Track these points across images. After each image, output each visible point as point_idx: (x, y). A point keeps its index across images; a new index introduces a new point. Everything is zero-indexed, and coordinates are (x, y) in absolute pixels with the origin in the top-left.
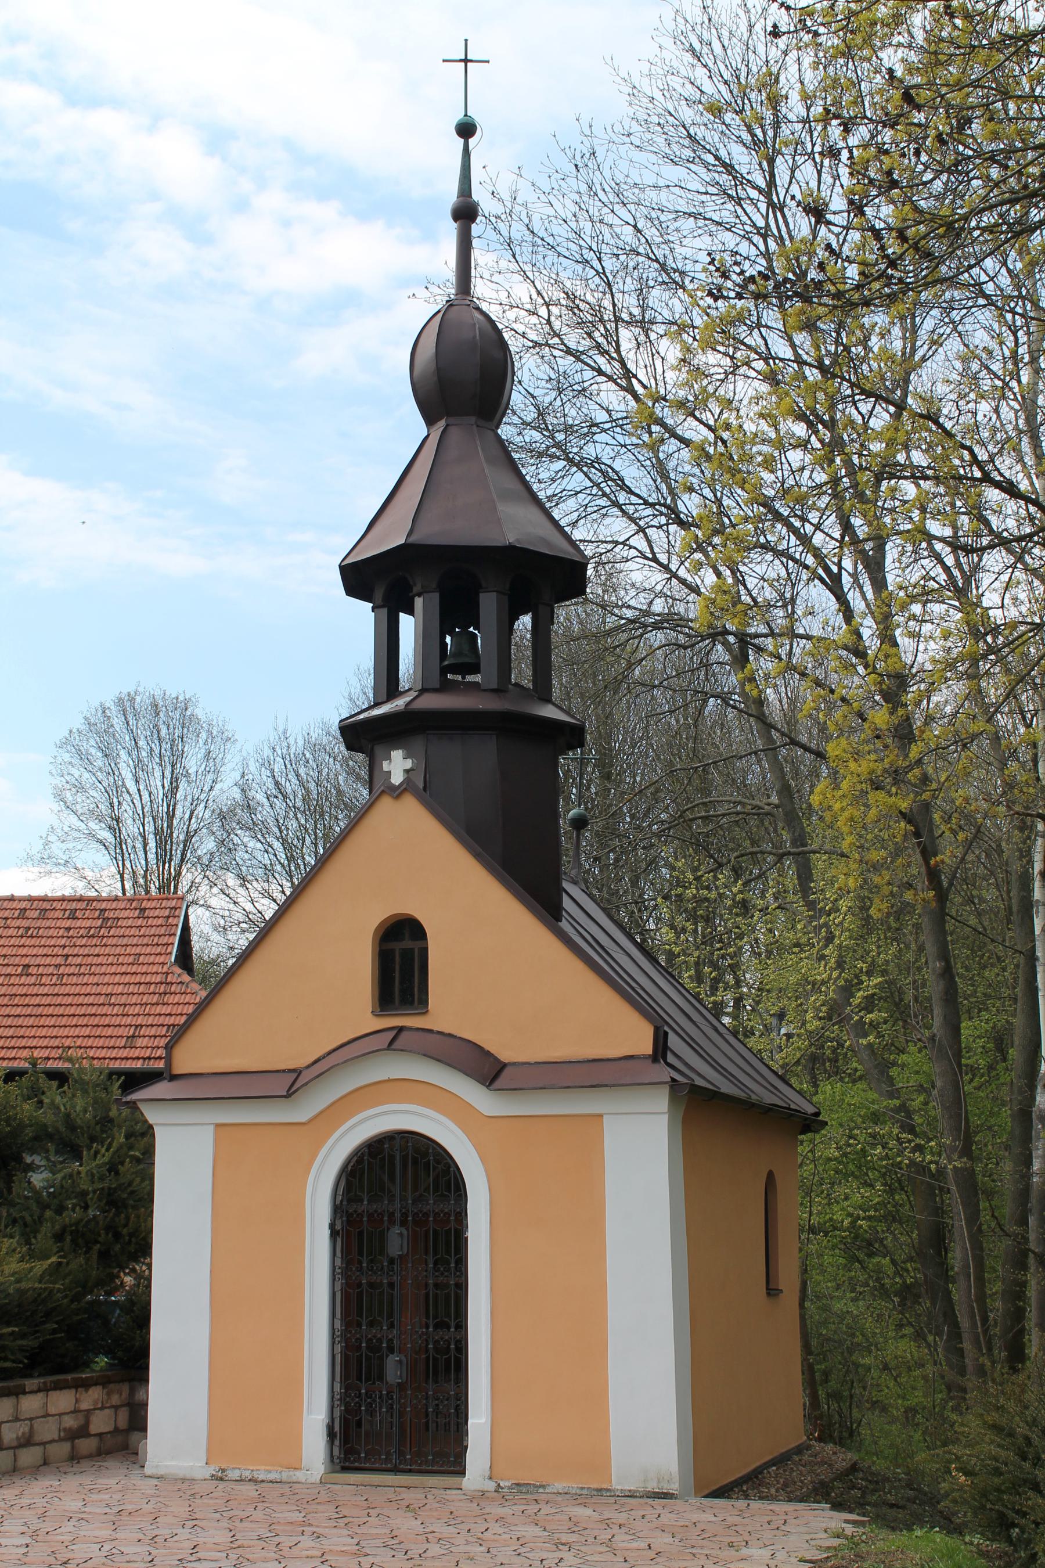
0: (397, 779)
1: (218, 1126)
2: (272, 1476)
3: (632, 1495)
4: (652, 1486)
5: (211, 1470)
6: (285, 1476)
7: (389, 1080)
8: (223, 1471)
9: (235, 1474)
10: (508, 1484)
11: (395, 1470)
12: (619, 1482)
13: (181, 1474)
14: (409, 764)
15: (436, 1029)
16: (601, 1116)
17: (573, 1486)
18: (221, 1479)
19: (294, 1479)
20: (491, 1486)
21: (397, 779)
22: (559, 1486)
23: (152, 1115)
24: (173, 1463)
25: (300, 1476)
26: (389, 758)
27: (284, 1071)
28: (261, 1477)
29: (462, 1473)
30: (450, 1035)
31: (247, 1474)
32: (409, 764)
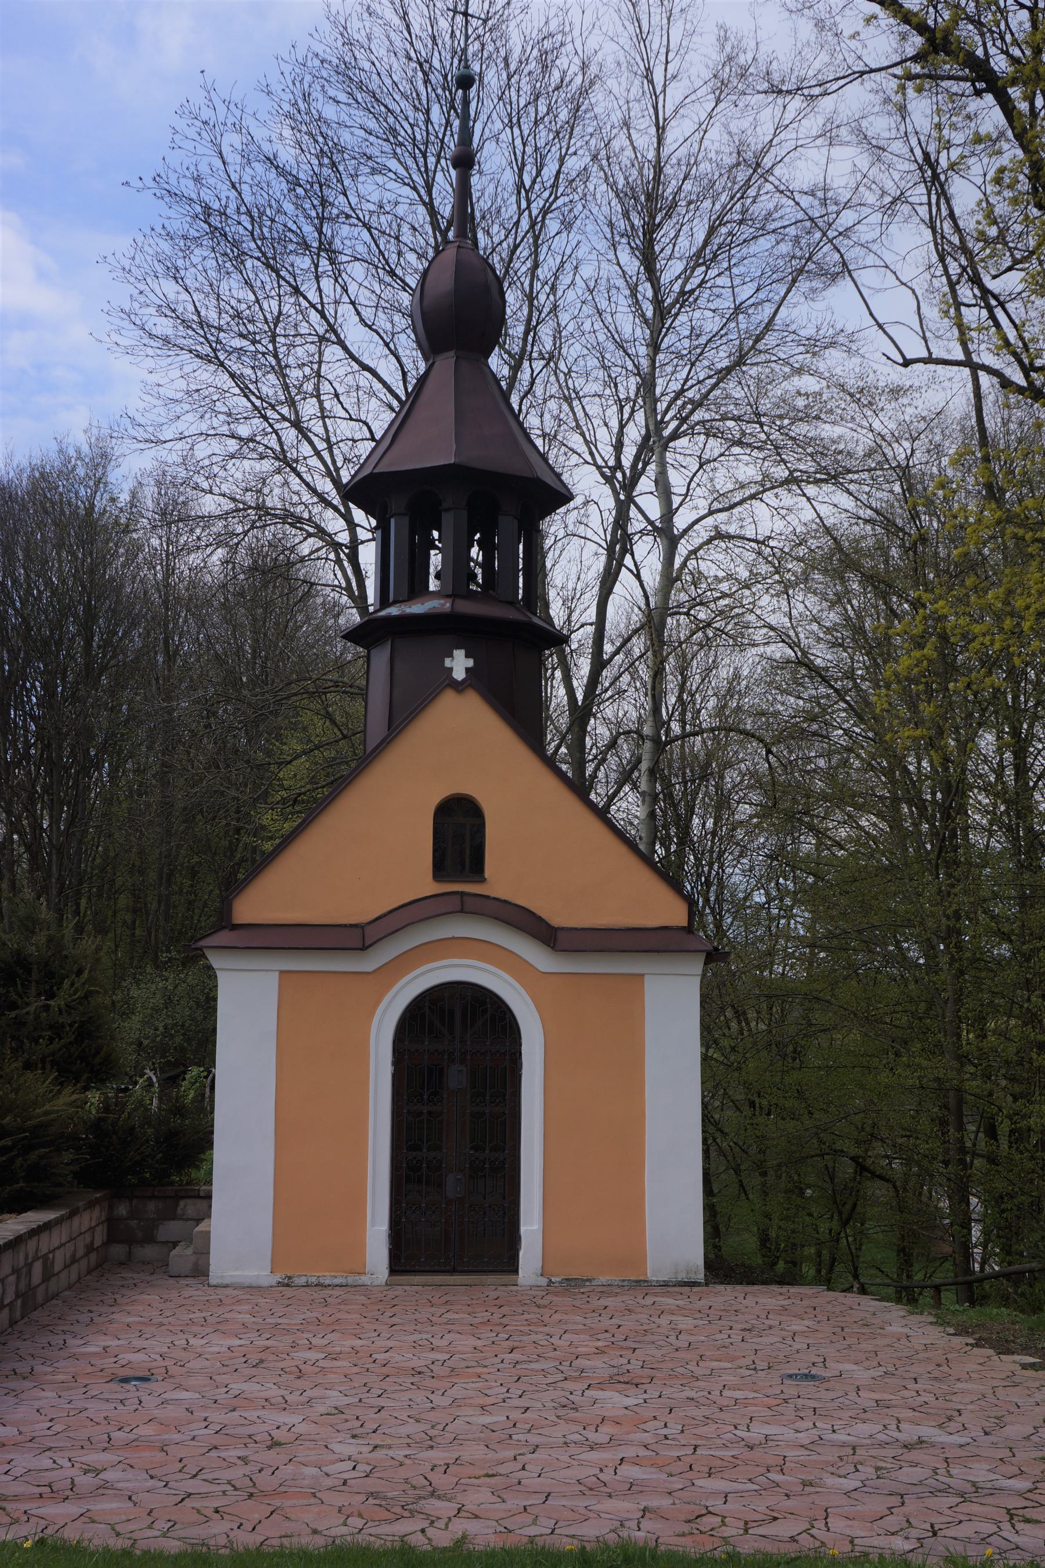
0: (459, 674)
1: (282, 972)
2: (337, 1281)
3: (665, 1284)
4: (682, 1276)
5: (277, 1278)
6: (350, 1280)
7: (454, 938)
8: (290, 1278)
9: (302, 1281)
10: (558, 1279)
11: (453, 1271)
12: (651, 1276)
13: (247, 1282)
14: (470, 663)
15: (493, 895)
16: (642, 975)
17: (615, 1278)
18: (288, 1285)
19: (360, 1282)
20: (543, 1281)
21: (459, 674)
22: (603, 1279)
23: (216, 961)
24: (238, 1273)
25: (365, 1279)
26: (451, 655)
27: (345, 926)
28: (327, 1282)
29: (516, 1271)
30: (505, 902)
31: (314, 1280)
32: (470, 663)
